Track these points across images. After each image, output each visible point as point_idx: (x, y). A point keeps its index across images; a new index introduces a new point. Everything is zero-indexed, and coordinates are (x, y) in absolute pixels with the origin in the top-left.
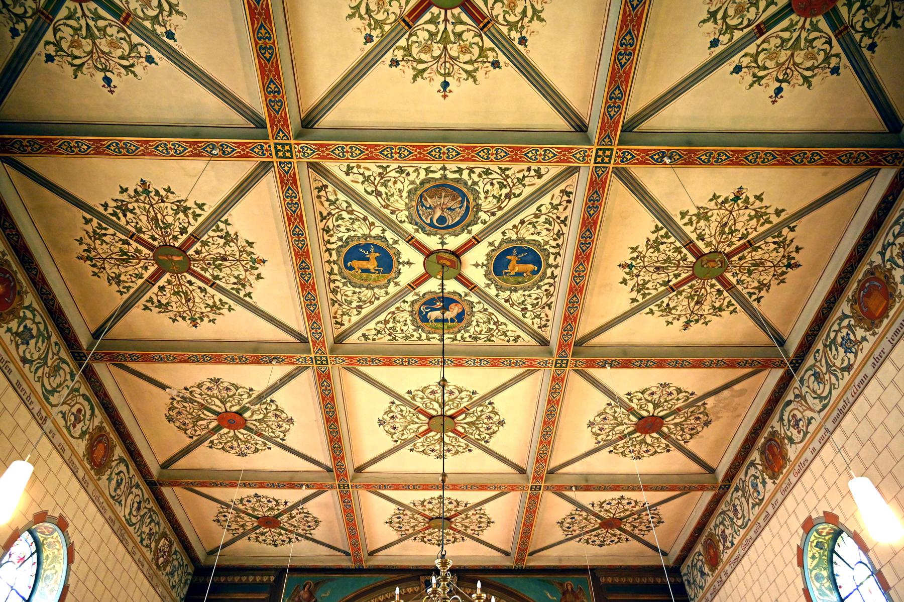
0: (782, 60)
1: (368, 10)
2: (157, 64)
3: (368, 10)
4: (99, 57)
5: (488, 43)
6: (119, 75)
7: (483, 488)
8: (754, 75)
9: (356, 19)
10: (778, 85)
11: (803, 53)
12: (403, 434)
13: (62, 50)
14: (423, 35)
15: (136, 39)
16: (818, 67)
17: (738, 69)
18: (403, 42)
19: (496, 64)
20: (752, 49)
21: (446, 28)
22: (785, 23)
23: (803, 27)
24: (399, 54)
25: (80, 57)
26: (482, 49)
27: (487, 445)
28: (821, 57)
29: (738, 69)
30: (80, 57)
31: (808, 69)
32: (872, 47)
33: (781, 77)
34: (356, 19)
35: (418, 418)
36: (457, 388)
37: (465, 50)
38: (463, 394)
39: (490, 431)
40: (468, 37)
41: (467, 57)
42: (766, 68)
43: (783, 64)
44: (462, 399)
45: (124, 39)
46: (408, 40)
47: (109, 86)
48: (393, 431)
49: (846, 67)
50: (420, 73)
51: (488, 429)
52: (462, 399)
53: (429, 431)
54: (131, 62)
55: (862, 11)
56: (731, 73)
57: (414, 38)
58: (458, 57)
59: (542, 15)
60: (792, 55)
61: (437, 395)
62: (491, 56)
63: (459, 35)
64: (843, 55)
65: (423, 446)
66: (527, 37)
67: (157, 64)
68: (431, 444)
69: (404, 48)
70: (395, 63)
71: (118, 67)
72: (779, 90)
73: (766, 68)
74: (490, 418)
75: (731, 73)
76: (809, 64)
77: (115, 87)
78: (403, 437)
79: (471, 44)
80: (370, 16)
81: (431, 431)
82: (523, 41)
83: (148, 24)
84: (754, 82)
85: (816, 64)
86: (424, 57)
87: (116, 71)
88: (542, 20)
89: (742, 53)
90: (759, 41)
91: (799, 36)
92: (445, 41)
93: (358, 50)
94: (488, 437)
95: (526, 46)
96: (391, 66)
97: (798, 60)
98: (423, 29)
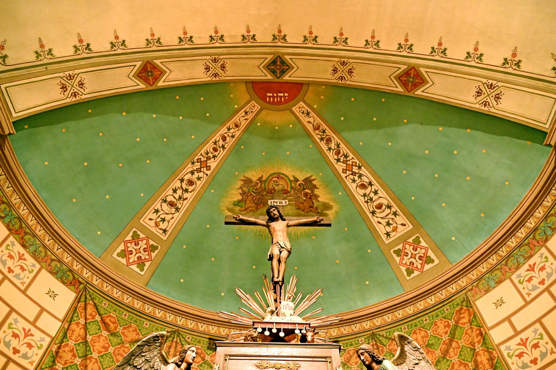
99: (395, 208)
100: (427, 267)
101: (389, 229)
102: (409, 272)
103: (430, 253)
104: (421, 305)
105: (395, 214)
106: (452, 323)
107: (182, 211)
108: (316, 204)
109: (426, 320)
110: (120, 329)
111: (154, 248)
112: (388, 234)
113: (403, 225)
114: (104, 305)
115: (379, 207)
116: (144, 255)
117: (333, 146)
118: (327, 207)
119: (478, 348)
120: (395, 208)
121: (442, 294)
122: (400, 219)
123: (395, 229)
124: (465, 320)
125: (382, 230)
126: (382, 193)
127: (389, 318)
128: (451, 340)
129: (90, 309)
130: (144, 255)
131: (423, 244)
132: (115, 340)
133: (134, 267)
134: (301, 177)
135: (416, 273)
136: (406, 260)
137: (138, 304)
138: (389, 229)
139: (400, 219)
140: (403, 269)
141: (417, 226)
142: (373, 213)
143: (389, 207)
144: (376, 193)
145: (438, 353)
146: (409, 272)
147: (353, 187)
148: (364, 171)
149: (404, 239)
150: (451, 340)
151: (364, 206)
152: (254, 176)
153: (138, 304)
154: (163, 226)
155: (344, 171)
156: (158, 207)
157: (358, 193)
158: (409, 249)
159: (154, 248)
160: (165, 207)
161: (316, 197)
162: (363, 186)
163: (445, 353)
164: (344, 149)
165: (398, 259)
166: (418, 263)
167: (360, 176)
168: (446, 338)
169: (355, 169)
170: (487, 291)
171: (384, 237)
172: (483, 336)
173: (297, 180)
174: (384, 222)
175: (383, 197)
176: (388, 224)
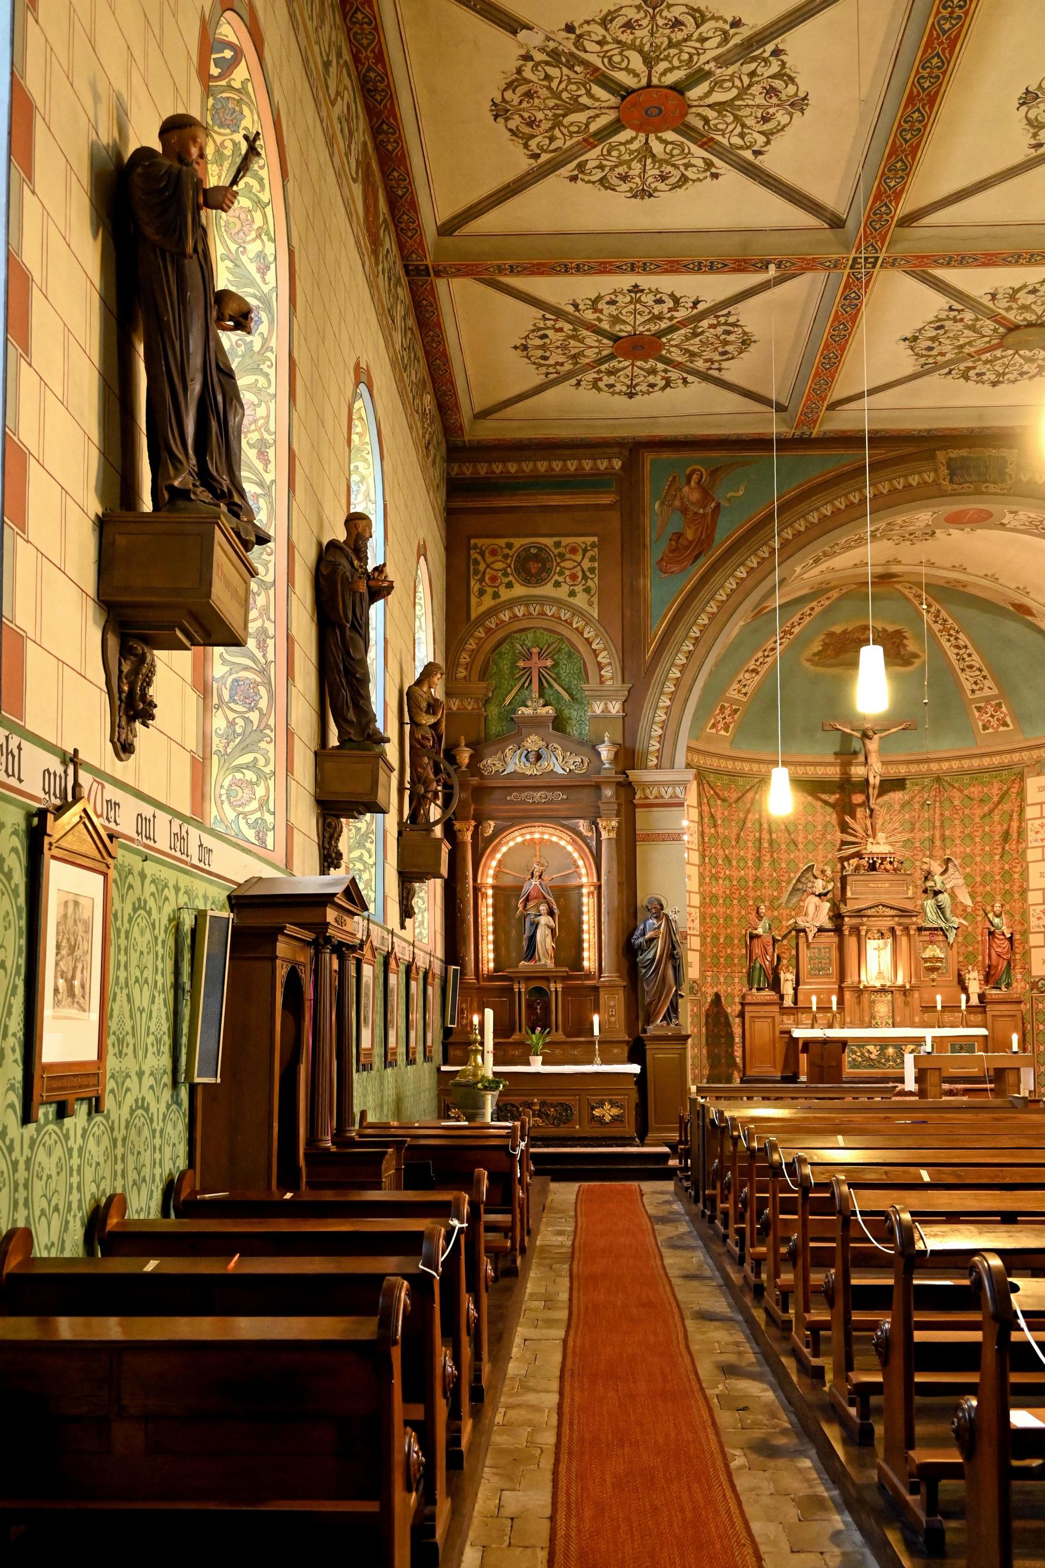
7: (741, 266)
12: (552, 139)
27: (757, 161)
35: (591, 96)
36: (693, 11)
38: (707, 28)
39: (767, 127)
44: (703, 40)
48: (527, 130)
51: (765, 119)
52: (703, 40)
53: (616, 126)
61: (639, 33)
65: (601, 167)
68: (621, 164)
74: (771, 91)
78: (553, 147)
81: (623, 128)
94: (761, 139)
99: (985, 673)
100: (1002, 729)
101: (975, 687)
102: (985, 728)
103: (1008, 720)
104: (986, 761)
105: (985, 677)
106: (1005, 788)
107: (761, 674)
108: (903, 652)
109: (986, 777)
110: (726, 794)
111: (736, 711)
112: (973, 691)
113: (989, 689)
114: (712, 778)
115: (971, 667)
116: (728, 720)
117: (932, 610)
118: (915, 656)
119: (1015, 816)
120: (985, 673)
121: (1006, 759)
122: (988, 683)
123: (981, 689)
124: (1014, 790)
125: (968, 686)
126: (975, 656)
127: (955, 765)
128: (999, 802)
129: (706, 786)
130: (728, 720)
131: (1004, 709)
132: (726, 804)
133: (722, 733)
134: (891, 628)
135: (991, 730)
136: (985, 717)
137: (730, 765)
138: (975, 687)
139: (988, 683)
140: (980, 724)
141: (1002, 694)
142: (963, 670)
143: (980, 670)
144: (970, 655)
145: (986, 809)
146: (985, 728)
147: (946, 645)
148: (961, 635)
149: (988, 700)
150: (999, 802)
151: (955, 663)
152: (838, 629)
153: (730, 765)
154: (744, 691)
155: (940, 631)
156: (741, 677)
157: (951, 653)
158: (990, 710)
159: (736, 711)
160: (747, 676)
161: (905, 646)
162: (958, 647)
163: (991, 811)
164: (944, 614)
165: (977, 714)
166: (994, 722)
167: (956, 639)
168: (996, 799)
169: (952, 632)
170: (1038, 775)
171: (969, 693)
172: (1022, 810)
173: (885, 630)
174: (972, 680)
175: (976, 660)
176: (976, 683)
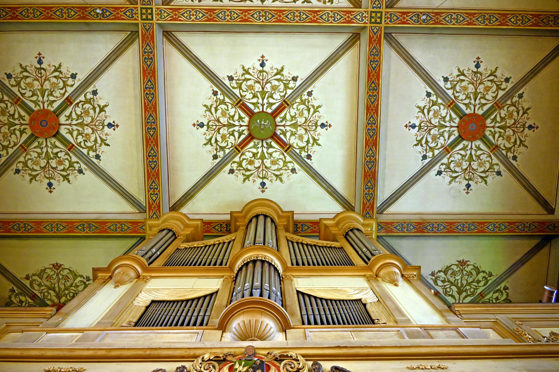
0: (464, 167)
1: (216, 141)
2: (84, 174)
3: (216, 141)
4: (49, 170)
5: (288, 159)
6: (59, 181)
8: (451, 177)
9: (209, 146)
10: (466, 182)
11: (476, 163)
13: (27, 166)
14: (249, 155)
15: (74, 159)
16: (487, 171)
17: (439, 173)
18: (237, 159)
19: (293, 171)
20: (445, 161)
21: (262, 150)
22: (461, 146)
23: (471, 148)
24: (235, 166)
25: (37, 171)
26: (285, 162)
28: (488, 165)
29: (439, 173)
30: (37, 171)
31: (482, 172)
32: (515, 158)
33: (467, 178)
34: (209, 146)
37: (274, 163)
40: (276, 155)
41: (275, 167)
42: (456, 172)
43: (466, 169)
45: (67, 159)
46: (240, 158)
47: (50, 188)
49: (504, 171)
50: (247, 178)
54: (68, 173)
55: (501, 138)
56: (436, 175)
57: (243, 157)
58: (270, 167)
59: (319, 142)
60: (470, 164)
62: (290, 166)
63: (271, 154)
64: (500, 164)
66: (311, 154)
67: (84, 174)
69: (237, 162)
70: (232, 171)
71: (59, 176)
72: (468, 186)
73: (456, 172)
75: (436, 175)
76: (482, 169)
77: (54, 188)
79: (278, 159)
80: (217, 144)
82: (309, 157)
83: (85, 151)
84: (452, 181)
85: (486, 170)
86: (249, 167)
87: (57, 179)
88: (319, 145)
89: (440, 164)
90: (448, 156)
91: (471, 153)
92: (263, 157)
93: (210, 164)
95: (311, 160)
96: (229, 173)
97: (475, 167)
98: (249, 151)
